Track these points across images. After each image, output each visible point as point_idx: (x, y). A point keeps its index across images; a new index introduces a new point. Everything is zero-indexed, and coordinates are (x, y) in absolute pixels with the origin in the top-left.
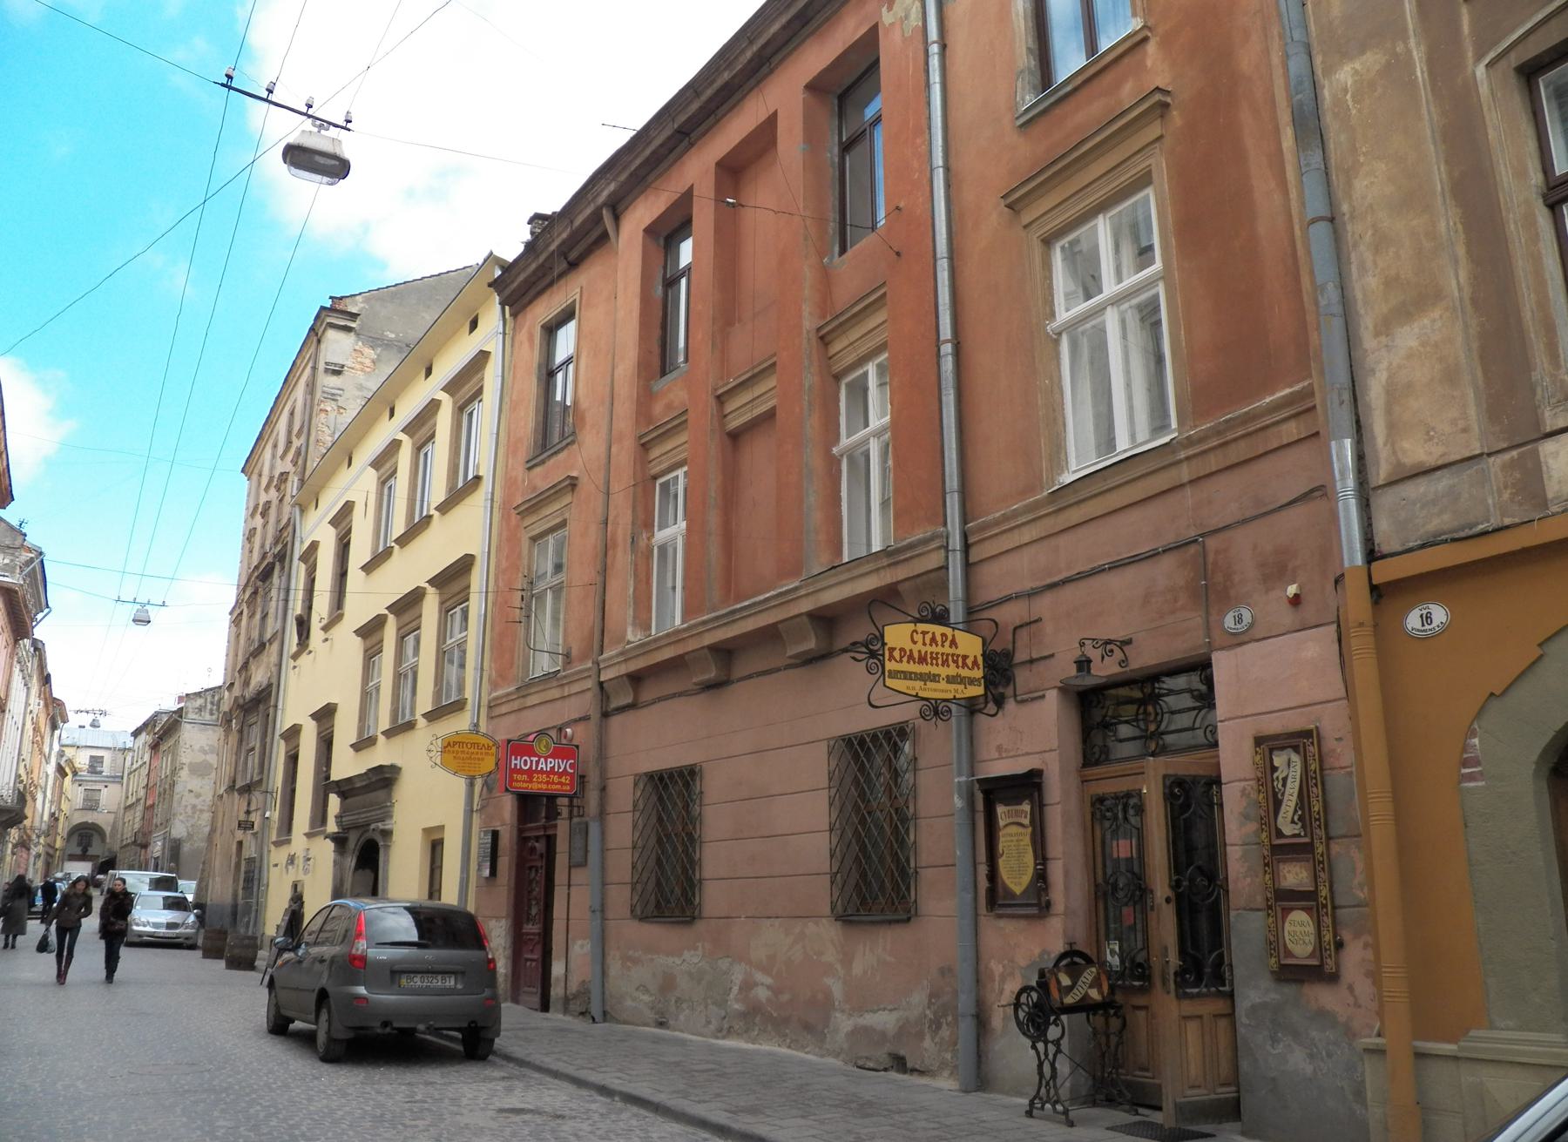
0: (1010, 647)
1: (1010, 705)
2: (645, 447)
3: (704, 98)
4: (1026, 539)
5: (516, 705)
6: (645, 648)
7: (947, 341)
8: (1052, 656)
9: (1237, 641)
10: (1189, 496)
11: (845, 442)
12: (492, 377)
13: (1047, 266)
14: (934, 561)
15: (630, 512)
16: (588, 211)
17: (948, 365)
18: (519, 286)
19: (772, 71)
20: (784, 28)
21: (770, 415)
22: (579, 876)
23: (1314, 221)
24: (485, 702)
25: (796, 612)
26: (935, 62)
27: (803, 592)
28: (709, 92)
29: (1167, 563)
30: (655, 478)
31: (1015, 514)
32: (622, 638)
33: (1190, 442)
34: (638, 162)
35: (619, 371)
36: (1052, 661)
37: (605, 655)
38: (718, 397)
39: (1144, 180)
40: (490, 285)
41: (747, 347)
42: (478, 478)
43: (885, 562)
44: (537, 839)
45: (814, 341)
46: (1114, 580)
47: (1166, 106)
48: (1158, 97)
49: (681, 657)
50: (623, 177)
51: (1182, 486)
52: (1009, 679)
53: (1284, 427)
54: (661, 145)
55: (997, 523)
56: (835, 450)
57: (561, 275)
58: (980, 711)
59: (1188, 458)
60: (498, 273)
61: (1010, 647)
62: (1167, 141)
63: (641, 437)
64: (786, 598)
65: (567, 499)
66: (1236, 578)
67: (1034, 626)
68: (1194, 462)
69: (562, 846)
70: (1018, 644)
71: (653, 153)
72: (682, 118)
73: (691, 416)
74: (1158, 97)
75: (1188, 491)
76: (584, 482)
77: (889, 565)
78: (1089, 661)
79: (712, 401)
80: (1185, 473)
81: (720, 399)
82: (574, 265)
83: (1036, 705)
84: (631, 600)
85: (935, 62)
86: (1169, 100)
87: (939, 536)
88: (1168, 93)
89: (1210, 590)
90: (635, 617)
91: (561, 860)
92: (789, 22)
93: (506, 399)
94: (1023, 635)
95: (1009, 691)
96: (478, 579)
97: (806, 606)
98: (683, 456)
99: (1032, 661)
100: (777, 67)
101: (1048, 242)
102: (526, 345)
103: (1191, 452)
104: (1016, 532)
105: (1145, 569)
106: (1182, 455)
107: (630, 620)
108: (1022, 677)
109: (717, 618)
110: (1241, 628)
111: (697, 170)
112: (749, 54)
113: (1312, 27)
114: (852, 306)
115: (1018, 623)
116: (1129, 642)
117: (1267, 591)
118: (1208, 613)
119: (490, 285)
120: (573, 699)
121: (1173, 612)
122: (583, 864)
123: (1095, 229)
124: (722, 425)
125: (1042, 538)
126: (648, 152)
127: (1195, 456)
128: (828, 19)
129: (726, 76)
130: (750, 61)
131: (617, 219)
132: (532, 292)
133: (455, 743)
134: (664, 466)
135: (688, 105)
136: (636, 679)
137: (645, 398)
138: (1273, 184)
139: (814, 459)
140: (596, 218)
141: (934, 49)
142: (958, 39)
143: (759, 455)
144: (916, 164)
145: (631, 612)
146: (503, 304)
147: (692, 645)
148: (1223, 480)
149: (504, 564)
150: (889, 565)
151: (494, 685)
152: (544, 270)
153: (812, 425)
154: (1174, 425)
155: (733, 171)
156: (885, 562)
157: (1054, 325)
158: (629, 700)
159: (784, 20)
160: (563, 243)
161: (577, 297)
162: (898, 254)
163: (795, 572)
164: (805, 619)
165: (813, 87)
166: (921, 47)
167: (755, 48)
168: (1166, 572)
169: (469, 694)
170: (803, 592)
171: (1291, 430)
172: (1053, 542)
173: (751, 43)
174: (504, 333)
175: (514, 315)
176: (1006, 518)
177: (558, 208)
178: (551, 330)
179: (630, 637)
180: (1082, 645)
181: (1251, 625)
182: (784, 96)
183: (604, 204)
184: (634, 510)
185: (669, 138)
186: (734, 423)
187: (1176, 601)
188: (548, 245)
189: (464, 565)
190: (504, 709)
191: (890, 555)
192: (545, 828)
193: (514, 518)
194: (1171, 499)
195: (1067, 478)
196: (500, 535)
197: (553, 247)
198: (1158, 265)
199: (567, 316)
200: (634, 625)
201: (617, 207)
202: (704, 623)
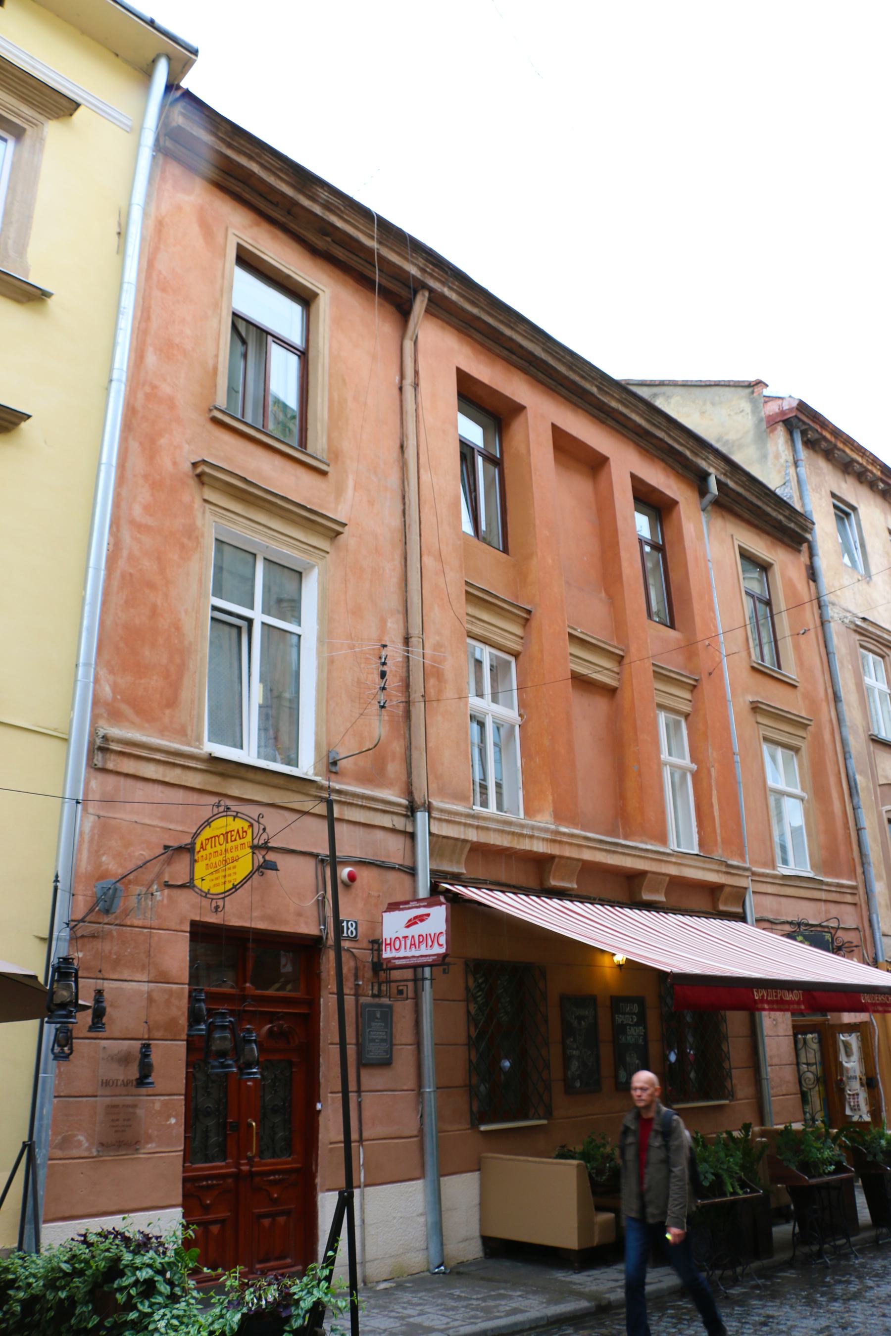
5: (194, 780)
19: (602, 422)
27: (673, 859)
43: (724, 869)
80: (823, 895)
97: (673, 871)
109: (601, 841)
112: (614, 404)
122: (386, 1063)
128: (647, 451)
147: (568, 852)
170: (673, 859)
171: (849, 898)
183: (431, 290)
190: (150, 771)
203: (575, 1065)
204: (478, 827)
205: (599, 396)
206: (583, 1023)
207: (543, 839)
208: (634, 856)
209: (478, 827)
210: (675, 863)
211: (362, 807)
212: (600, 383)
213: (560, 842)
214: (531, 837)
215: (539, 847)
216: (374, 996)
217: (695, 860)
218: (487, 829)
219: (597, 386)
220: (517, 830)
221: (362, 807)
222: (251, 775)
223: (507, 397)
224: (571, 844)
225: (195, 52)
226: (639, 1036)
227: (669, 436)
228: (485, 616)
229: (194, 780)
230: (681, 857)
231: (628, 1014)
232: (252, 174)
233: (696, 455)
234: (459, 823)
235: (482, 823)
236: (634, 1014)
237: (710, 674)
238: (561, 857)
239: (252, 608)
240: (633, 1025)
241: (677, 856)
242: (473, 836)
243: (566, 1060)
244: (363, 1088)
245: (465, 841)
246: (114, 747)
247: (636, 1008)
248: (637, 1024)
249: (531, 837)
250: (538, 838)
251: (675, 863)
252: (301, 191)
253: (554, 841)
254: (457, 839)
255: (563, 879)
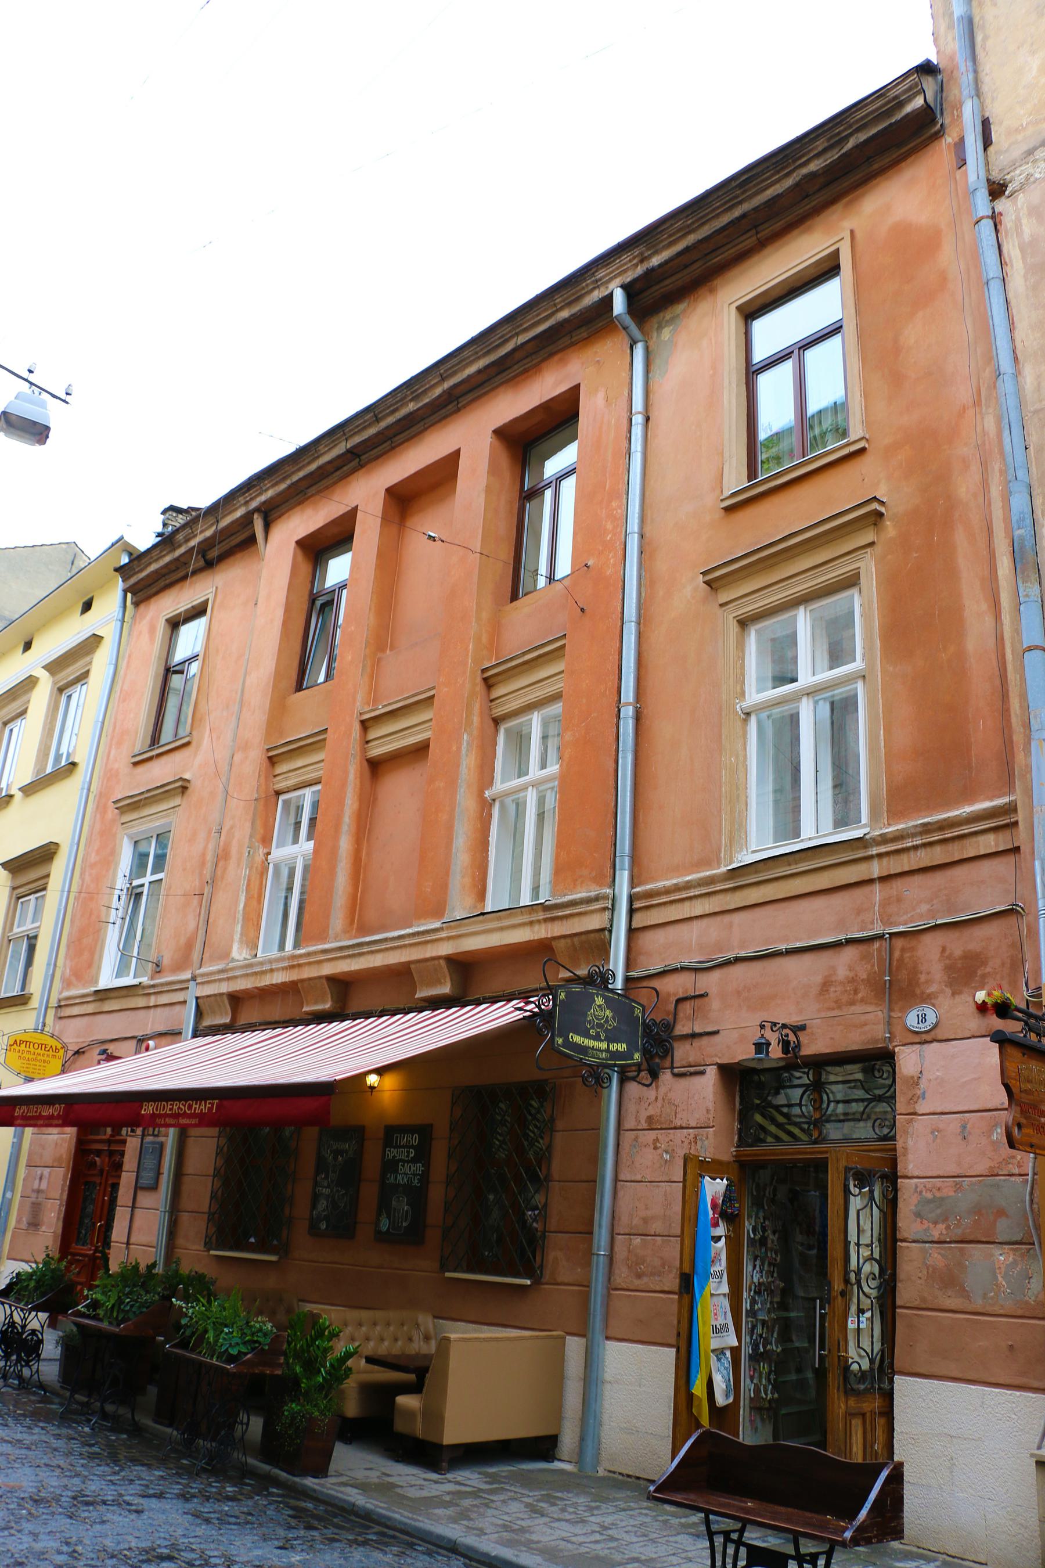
0: (671, 1018)
1: (666, 1077)
2: (272, 761)
3: (383, 424)
4: (698, 912)
5: (90, 1008)
6: (250, 969)
7: (628, 704)
8: (716, 1033)
9: (923, 1038)
10: (877, 892)
11: (500, 786)
12: (101, 663)
13: (741, 646)
14: (594, 922)
15: (248, 825)
16: (238, 514)
17: (627, 727)
18: (148, 576)
19: (458, 410)
20: (479, 372)
21: (421, 750)
22: (145, 1199)
23: (1030, 649)
24: (53, 1002)
25: (434, 954)
26: (637, 431)
27: (444, 934)
28: (391, 420)
29: (849, 953)
30: (278, 793)
31: (688, 886)
32: (226, 955)
33: (884, 839)
34: (301, 474)
35: (253, 679)
36: (716, 1039)
37: (203, 970)
38: (363, 723)
39: (852, 581)
40: (116, 570)
41: (401, 680)
42: (74, 764)
43: (541, 916)
44: (98, 1153)
45: (479, 680)
46: (790, 964)
47: (881, 515)
48: (875, 506)
49: (294, 983)
50: (283, 486)
51: (871, 881)
52: (667, 1052)
53: (981, 839)
54: (330, 462)
55: (667, 891)
56: (487, 794)
57: (194, 573)
58: (634, 1079)
59: (880, 856)
60: (125, 560)
61: (671, 1018)
62: (878, 549)
63: (268, 750)
64: (424, 938)
65: (177, 801)
66: (923, 978)
67: (698, 1001)
68: (885, 860)
69: (130, 1162)
70: (681, 1015)
71: (320, 468)
72: (357, 439)
73: (329, 735)
74: (875, 506)
75: (877, 887)
76: (196, 786)
77: (545, 920)
78: (769, 1044)
79: (357, 727)
80: (876, 869)
81: (365, 725)
82: (210, 565)
83: (697, 1080)
84: (240, 916)
85: (637, 431)
86: (883, 510)
87: (605, 897)
88: (883, 503)
89: (897, 988)
90: (241, 934)
91: (127, 1179)
92: (487, 367)
93: (117, 688)
94: (687, 1007)
95: (668, 1063)
96: (58, 870)
97: (446, 949)
98: (315, 775)
99: (694, 1036)
100: (464, 407)
101: (744, 623)
102: (145, 637)
103: (883, 849)
104: (687, 904)
105: (825, 956)
106: (874, 851)
107: (237, 937)
108: (682, 1053)
109: (341, 948)
110: (924, 1027)
111: (366, 493)
112: (438, 391)
113: (1034, 469)
114: (524, 654)
115: (681, 995)
116: (803, 1028)
117: (953, 994)
118: (891, 1010)
119: (116, 570)
120: (159, 1010)
121: (852, 1003)
122: (154, 1187)
123: (795, 618)
124: (364, 751)
125: (715, 914)
126: (313, 467)
127: (888, 854)
129: (412, 407)
130: (440, 396)
131: (267, 527)
132: (162, 583)
133: (22, 1042)
134: (290, 783)
135: (365, 428)
136: (236, 1000)
137: (278, 711)
138: (984, 606)
139: (465, 801)
140: (247, 521)
141: (638, 419)
142: (662, 414)
143: (401, 789)
144: (609, 526)
145: (238, 928)
146: (125, 592)
147: (307, 973)
148: (917, 879)
149: (93, 858)
150: (545, 920)
151: (67, 984)
152: (179, 563)
153: (468, 763)
154: (864, 820)
155: (404, 501)
156: (541, 916)
157: (744, 705)
158: (227, 1020)
159: (481, 363)
160: (206, 540)
161: (211, 597)
162: (582, 610)
163: (438, 911)
164: (442, 962)
165: (499, 433)
166: (625, 415)
167: (446, 385)
168: (844, 962)
169: (36, 986)
171: (989, 843)
172: (727, 918)
173: (443, 380)
174: (123, 621)
175: (136, 604)
176: (677, 888)
177: (204, 502)
178: (175, 624)
179: (235, 954)
180: (762, 1027)
181: (935, 1026)
182: (471, 438)
183: (257, 510)
184: (253, 824)
185: (339, 457)
186: (377, 750)
187: (856, 991)
188: (187, 540)
189: (46, 854)
190: (76, 1010)
191: (549, 911)
192: (109, 1142)
193: (111, 812)
194: (859, 893)
195: (748, 858)
196: (92, 828)
197: (193, 543)
198: (857, 665)
199: (198, 612)
200: (241, 942)
201: (270, 514)
202: (325, 951)
203: (323, 1204)
204: (228, 979)
205: (420, 404)
206: (340, 1158)
207: (283, 969)
208: (387, 949)
209: (228, 979)
210: (449, 938)
211: (168, 991)
212: (412, 393)
213: (299, 965)
214: (272, 970)
215: (279, 978)
216: (153, 1135)
217: (481, 922)
218: (236, 977)
219: (411, 400)
220: (257, 969)
221: (168, 991)
222: (112, 995)
223: (341, 516)
224: (310, 963)
225: (121, 538)
226: (415, 1175)
227: (526, 330)
228: (299, 763)
229: (90, 1008)
230: (455, 927)
231: (403, 1147)
232: (156, 572)
233: (578, 299)
234: (215, 981)
235: (230, 974)
236: (412, 1147)
237: (582, 610)
238: (302, 981)
239: (152, 874)
240: (408, 1162)
241: (448, 928)
242: (224, 988)
243: (315, 1198)
244: (137, 1205)
245: (221, 995)
246: (62, 1003)
247: (415, 1139)
248: (414, 1160)
249: (272, 970)
250: (278, 969)
251: (449, 938)
252: (174, 550)
253: (292, 967)
254: (215, 995)
255: (316, 1003)
